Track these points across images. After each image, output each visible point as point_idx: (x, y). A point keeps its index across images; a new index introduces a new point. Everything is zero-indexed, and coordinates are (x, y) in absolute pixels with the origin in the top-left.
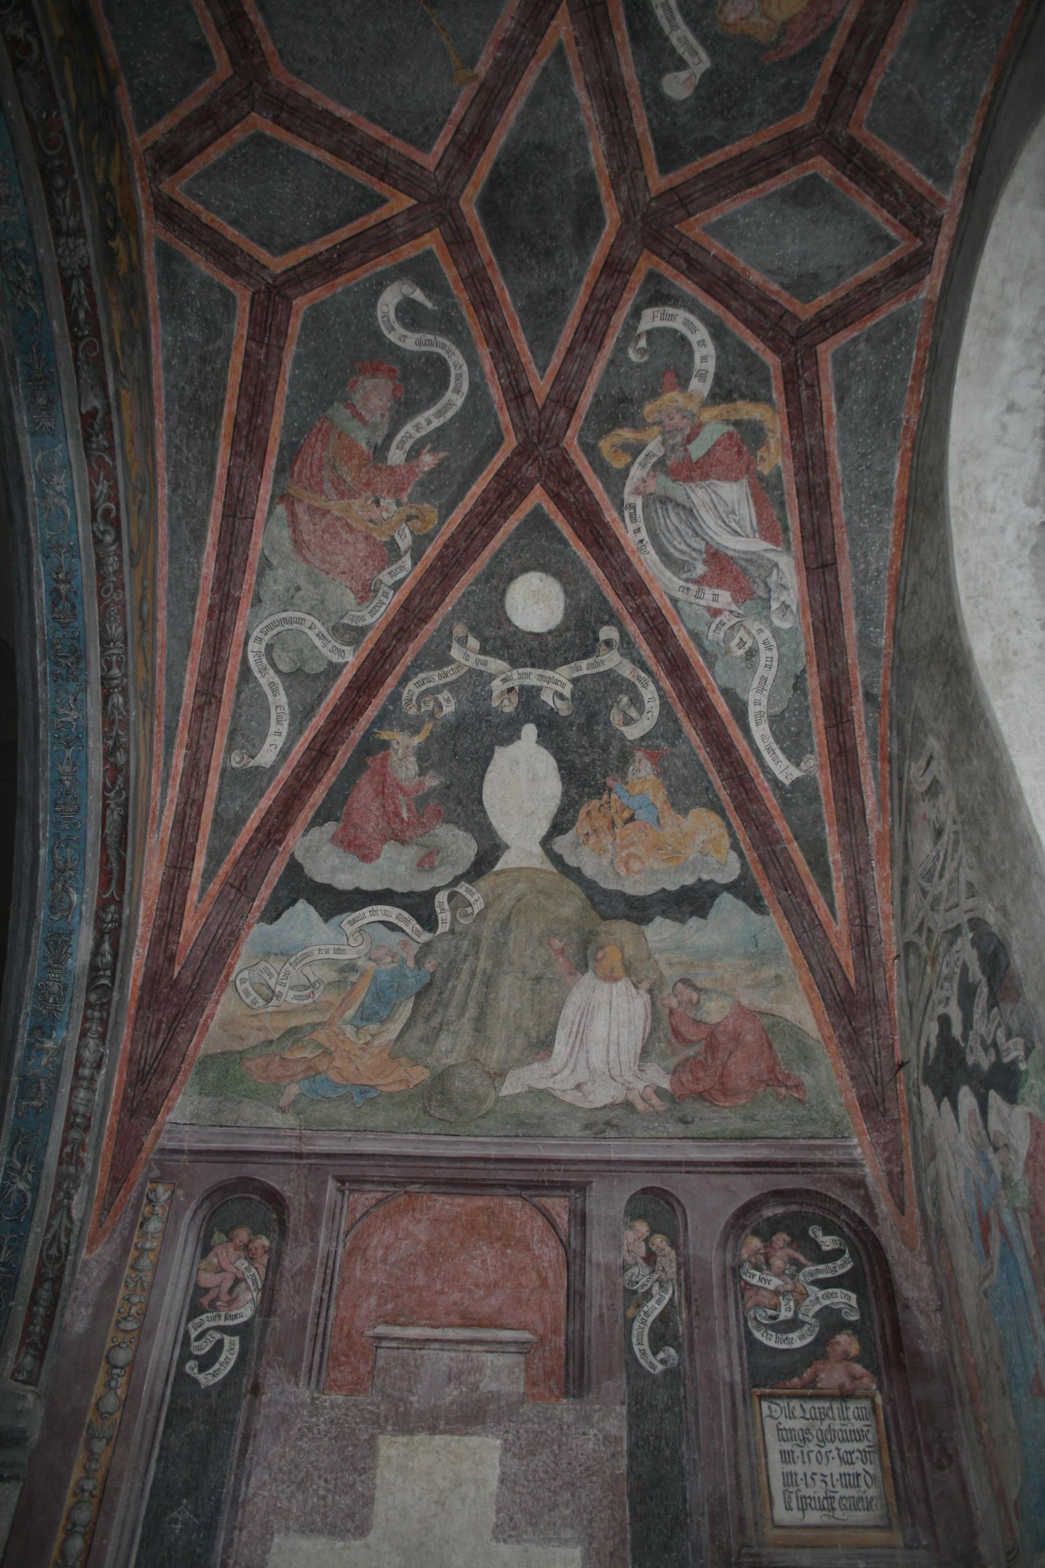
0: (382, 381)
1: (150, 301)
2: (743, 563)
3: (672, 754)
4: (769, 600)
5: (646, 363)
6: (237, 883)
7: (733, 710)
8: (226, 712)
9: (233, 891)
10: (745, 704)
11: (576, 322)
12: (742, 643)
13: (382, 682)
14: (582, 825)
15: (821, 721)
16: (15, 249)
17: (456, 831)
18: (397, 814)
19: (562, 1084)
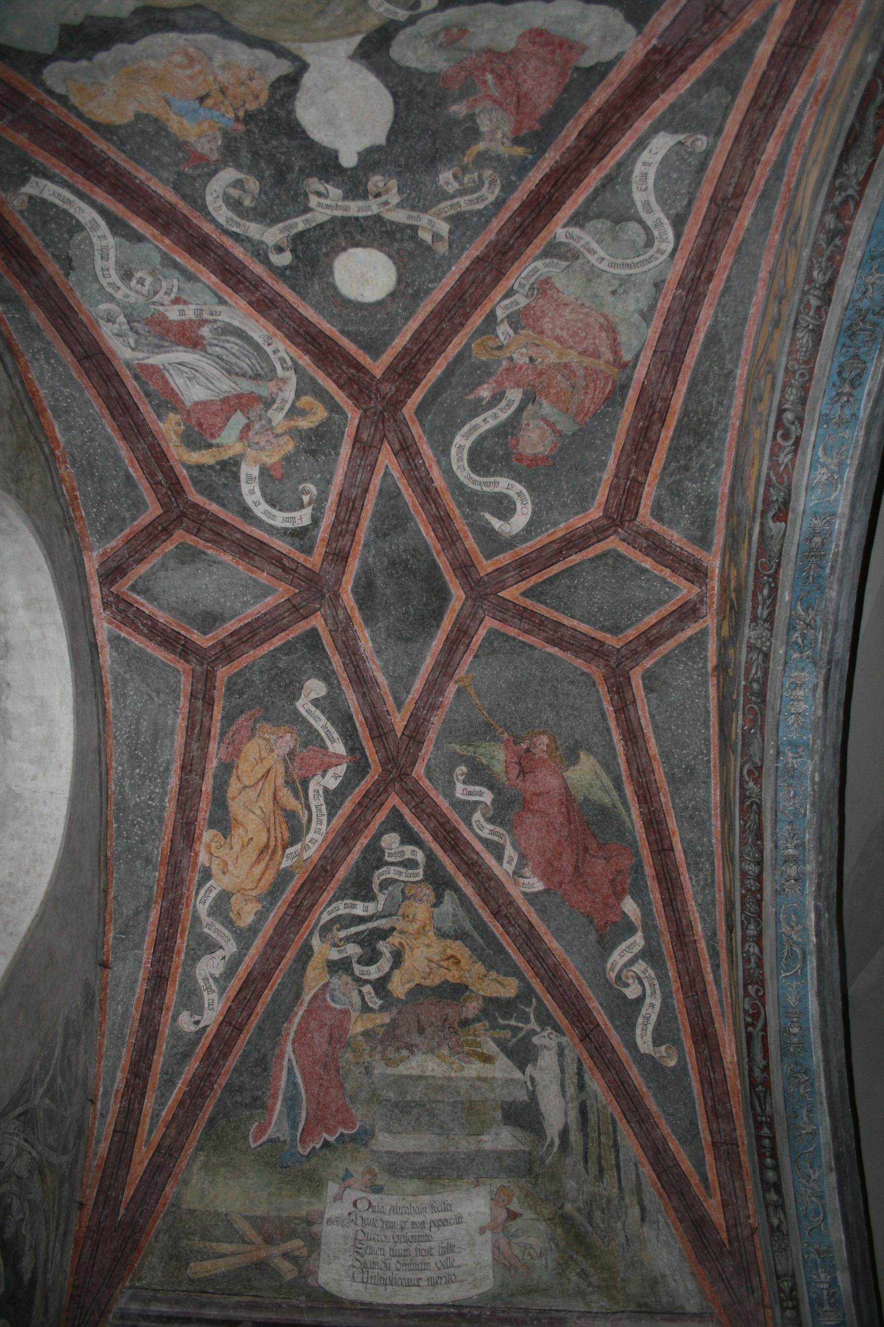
0: (528, 451)
1: (725, 510)
2: (166, 344)
3: (177, 165)
4: (129, 322)
5: (300, 483)
6: (718, 16)
7: (125, 225)
8: (707, 190)
9: (725, 8)
10: (115, 234)
11: (363, 515)
12: (141, 282)
13: (524, 205)
14: (261, 86)
15: (26, 240)
16: (801, 652)
17: (420, 66)
18: (500, 78)
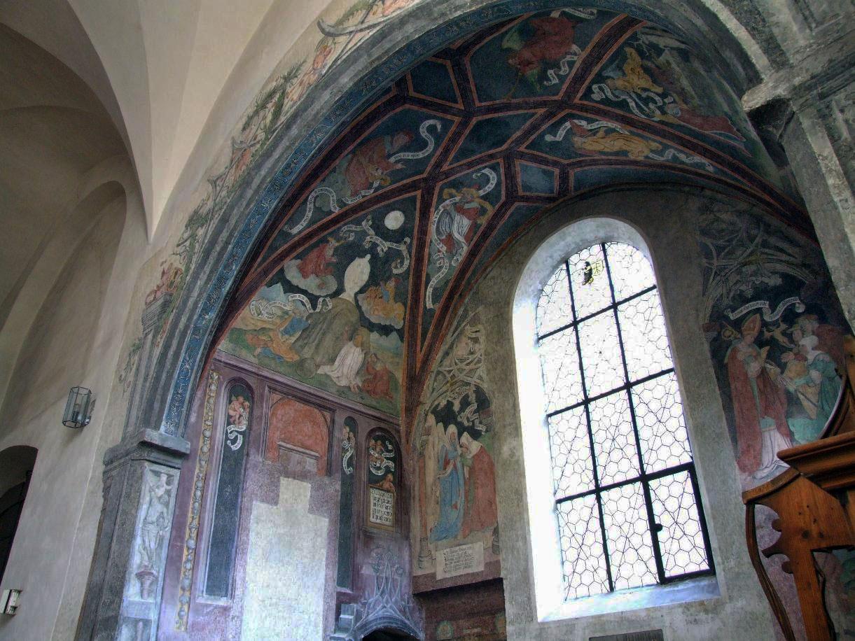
18: (320, 266)
19: (334, 375)
